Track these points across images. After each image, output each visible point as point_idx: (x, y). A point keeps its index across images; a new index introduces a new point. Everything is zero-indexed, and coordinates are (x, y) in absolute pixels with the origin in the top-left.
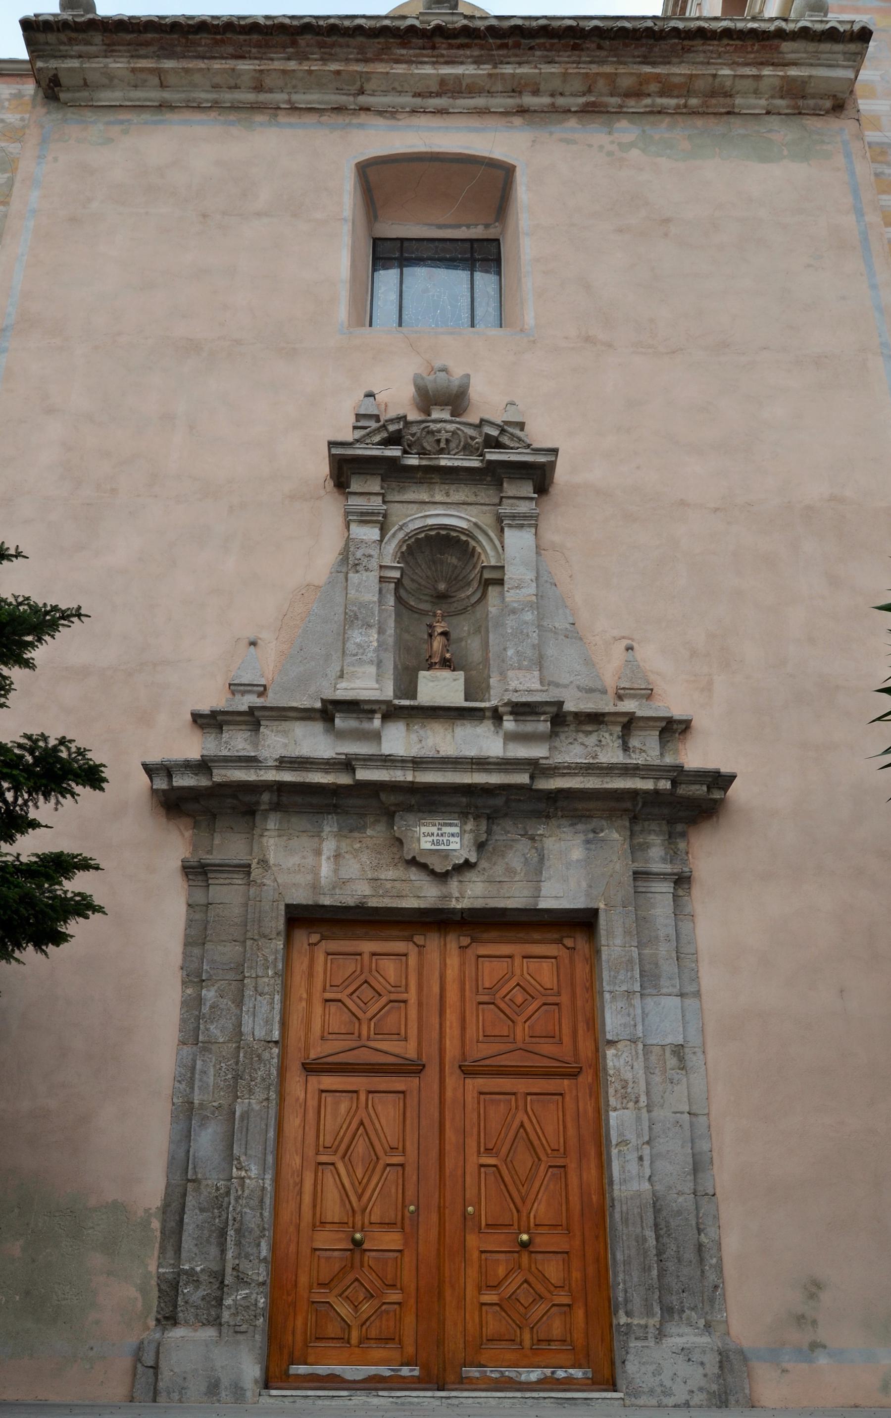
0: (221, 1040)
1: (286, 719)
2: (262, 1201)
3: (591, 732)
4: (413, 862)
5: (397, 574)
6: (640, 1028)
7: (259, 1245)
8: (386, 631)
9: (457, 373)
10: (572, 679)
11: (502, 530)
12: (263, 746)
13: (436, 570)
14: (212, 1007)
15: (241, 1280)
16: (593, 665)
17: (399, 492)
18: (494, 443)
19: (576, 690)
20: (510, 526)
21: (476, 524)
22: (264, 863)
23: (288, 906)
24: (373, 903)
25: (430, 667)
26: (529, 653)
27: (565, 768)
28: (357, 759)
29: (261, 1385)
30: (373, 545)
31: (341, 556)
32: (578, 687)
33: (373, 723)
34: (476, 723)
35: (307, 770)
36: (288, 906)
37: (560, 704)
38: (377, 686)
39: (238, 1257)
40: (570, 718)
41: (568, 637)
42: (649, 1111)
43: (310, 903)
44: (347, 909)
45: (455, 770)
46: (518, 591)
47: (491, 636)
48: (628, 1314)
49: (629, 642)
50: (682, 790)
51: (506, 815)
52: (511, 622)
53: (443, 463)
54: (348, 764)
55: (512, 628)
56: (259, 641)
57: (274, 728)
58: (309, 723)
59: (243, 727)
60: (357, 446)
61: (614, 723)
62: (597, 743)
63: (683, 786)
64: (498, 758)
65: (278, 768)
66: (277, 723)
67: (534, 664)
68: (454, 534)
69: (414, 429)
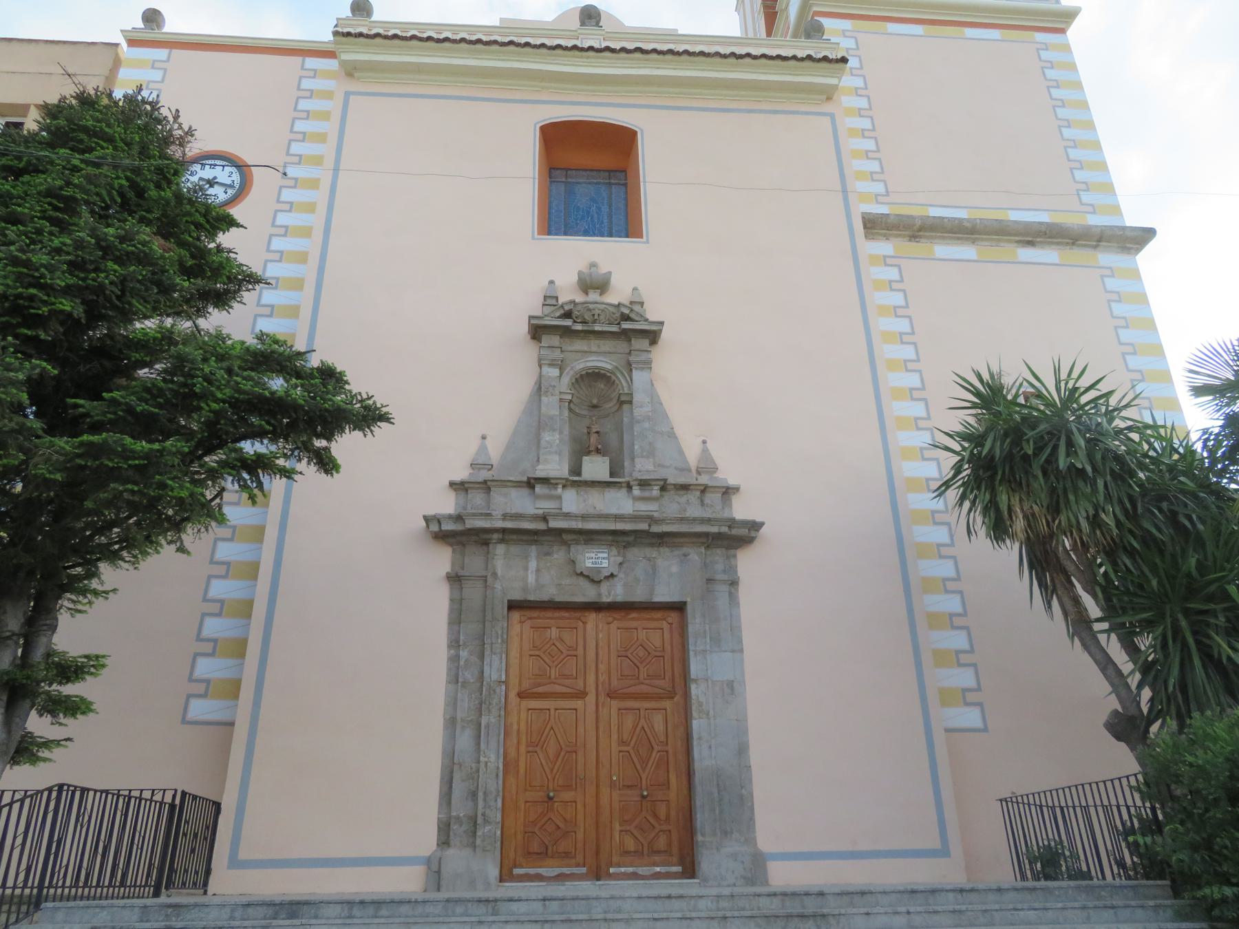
0: (472, 681)
1: (506, 486)
2: (497, 775)
3: (682, 495)
4: (581, 574)
5: (569, 397)
6: (709, 672)
7: (496, 800)
9: (603, 270)
11: (631, 370)
14: (466, 661)
15: (486, 821)
18: (626, 318)
20: (636, 369)
21: (617, 368)
22: (495, 574)
23: (508, 601)
24: (558, 599)
25: (588, 453)
29: (498, 880)
32: (676, 468)
36: (508, 601)
37: (665, 480)
38: (559, 468)
39: (485, 807)
42: (715, 719)
43: (522, 599)
44: (544, 602)
48: (703, 835)
49: (703, 438)
50: (734, 532)
51: (634, 546)
54: (544, 518)
58: (519, 489)
59: (480, 491)
60: (546, 318)
63: (735, 529)
68: (602, 372)
69: (579, 308)
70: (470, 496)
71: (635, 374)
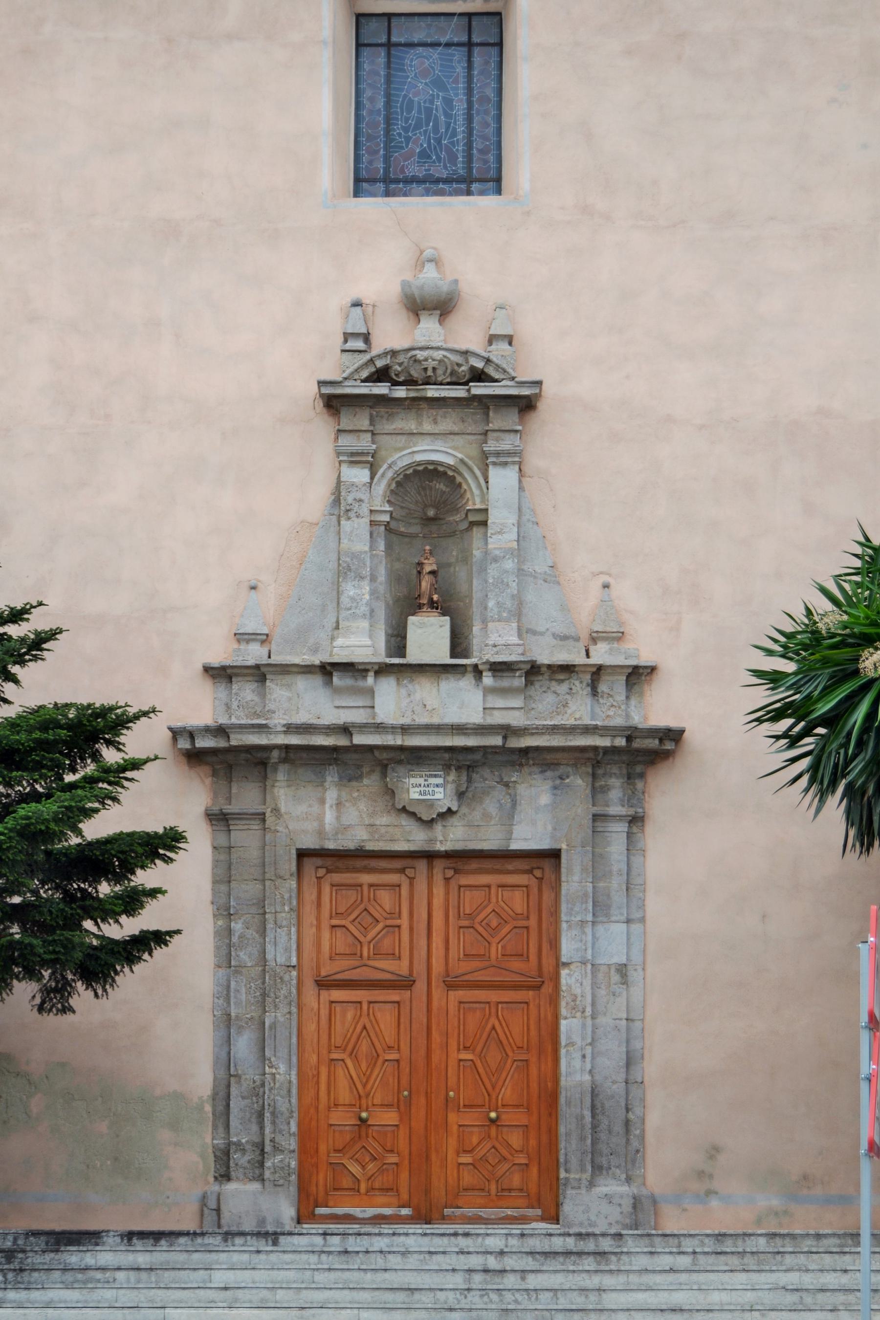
3: (562, 681)
5: (386, 518)
8: (377, 578)
10: (548, 626)
12: (270, 700)
13: (426, 495)
16: (569, 611)
17: (388, 420)
19: (551, 637)
20: (494, 464)
21: (462, 460)
26: (509, 604)
27: (533, 729)
28: (353, 726)
30: (364, 487)
31: (333, 497)
33: (366, 680)
34: (459, 676)
35: (310, 733)
38: (369, 643)
40: (544, 669)
41: (546, 582)
45: (438, 734)
46: (500, 537)
47: (475, 582)
52: (493, 571)
53: (430, 394)
55: (494, 578)
56: (259, 584)
57: (279, 682)
58: (309, 676)
61: (585, 672)
62: (568, 691)
64: (474, 724)
65: (285, 732)
66: (280, 677)
67: (513, 615)
68: (441, 469)
70: (235, 687)
71: (492, 471)
